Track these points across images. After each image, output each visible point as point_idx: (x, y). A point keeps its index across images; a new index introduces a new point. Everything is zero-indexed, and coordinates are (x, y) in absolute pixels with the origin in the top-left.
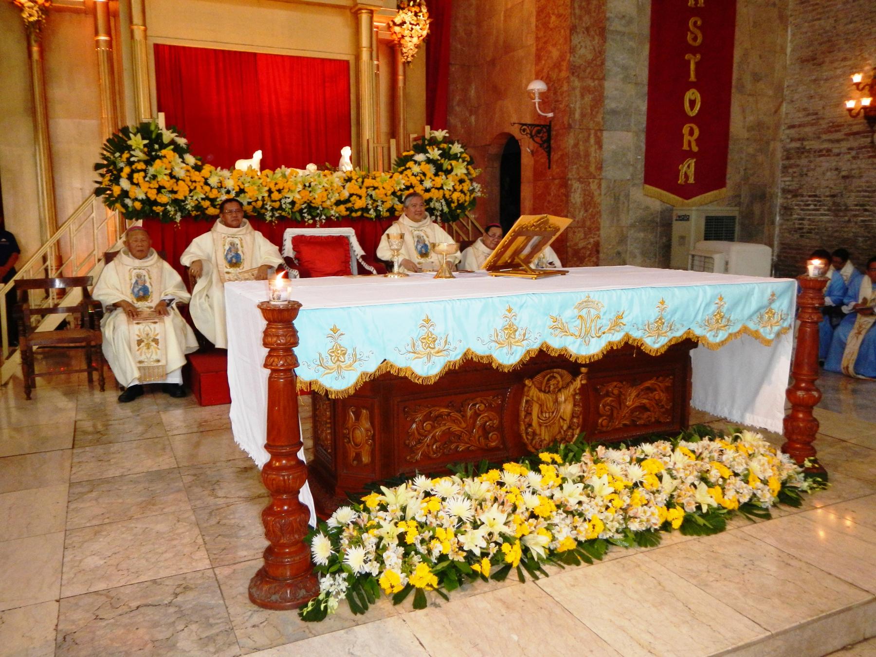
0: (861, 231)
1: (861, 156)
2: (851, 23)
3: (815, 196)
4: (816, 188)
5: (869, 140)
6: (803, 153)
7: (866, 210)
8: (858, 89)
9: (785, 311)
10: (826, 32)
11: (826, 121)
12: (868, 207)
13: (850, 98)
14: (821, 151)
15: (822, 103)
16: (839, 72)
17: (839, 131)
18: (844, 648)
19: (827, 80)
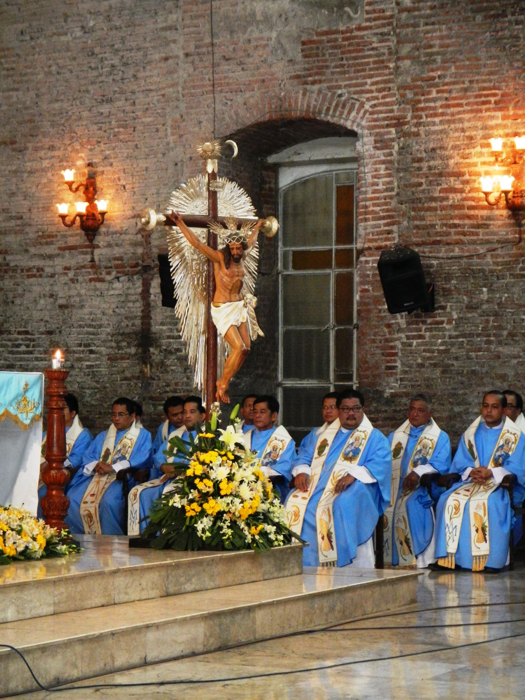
0: (89, 381)
1: (80, 278)
2: (57, 101)
3: (27, 333)
4: (27, 322)
5: (89, 257)
6: (6, 271)
7: (91, 352)
8: (71, 189)
9: (36, 400)
10: (26, 108)
11: (34, 229)
12: (94, 348)
13: (61, 201)
14: (29, 270)
15: (27, 203)
16: (46, 164)
17: (52, 243)
18: (103, 606)
19: (31, 172)
